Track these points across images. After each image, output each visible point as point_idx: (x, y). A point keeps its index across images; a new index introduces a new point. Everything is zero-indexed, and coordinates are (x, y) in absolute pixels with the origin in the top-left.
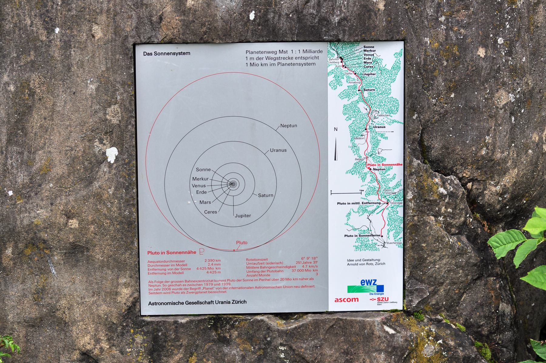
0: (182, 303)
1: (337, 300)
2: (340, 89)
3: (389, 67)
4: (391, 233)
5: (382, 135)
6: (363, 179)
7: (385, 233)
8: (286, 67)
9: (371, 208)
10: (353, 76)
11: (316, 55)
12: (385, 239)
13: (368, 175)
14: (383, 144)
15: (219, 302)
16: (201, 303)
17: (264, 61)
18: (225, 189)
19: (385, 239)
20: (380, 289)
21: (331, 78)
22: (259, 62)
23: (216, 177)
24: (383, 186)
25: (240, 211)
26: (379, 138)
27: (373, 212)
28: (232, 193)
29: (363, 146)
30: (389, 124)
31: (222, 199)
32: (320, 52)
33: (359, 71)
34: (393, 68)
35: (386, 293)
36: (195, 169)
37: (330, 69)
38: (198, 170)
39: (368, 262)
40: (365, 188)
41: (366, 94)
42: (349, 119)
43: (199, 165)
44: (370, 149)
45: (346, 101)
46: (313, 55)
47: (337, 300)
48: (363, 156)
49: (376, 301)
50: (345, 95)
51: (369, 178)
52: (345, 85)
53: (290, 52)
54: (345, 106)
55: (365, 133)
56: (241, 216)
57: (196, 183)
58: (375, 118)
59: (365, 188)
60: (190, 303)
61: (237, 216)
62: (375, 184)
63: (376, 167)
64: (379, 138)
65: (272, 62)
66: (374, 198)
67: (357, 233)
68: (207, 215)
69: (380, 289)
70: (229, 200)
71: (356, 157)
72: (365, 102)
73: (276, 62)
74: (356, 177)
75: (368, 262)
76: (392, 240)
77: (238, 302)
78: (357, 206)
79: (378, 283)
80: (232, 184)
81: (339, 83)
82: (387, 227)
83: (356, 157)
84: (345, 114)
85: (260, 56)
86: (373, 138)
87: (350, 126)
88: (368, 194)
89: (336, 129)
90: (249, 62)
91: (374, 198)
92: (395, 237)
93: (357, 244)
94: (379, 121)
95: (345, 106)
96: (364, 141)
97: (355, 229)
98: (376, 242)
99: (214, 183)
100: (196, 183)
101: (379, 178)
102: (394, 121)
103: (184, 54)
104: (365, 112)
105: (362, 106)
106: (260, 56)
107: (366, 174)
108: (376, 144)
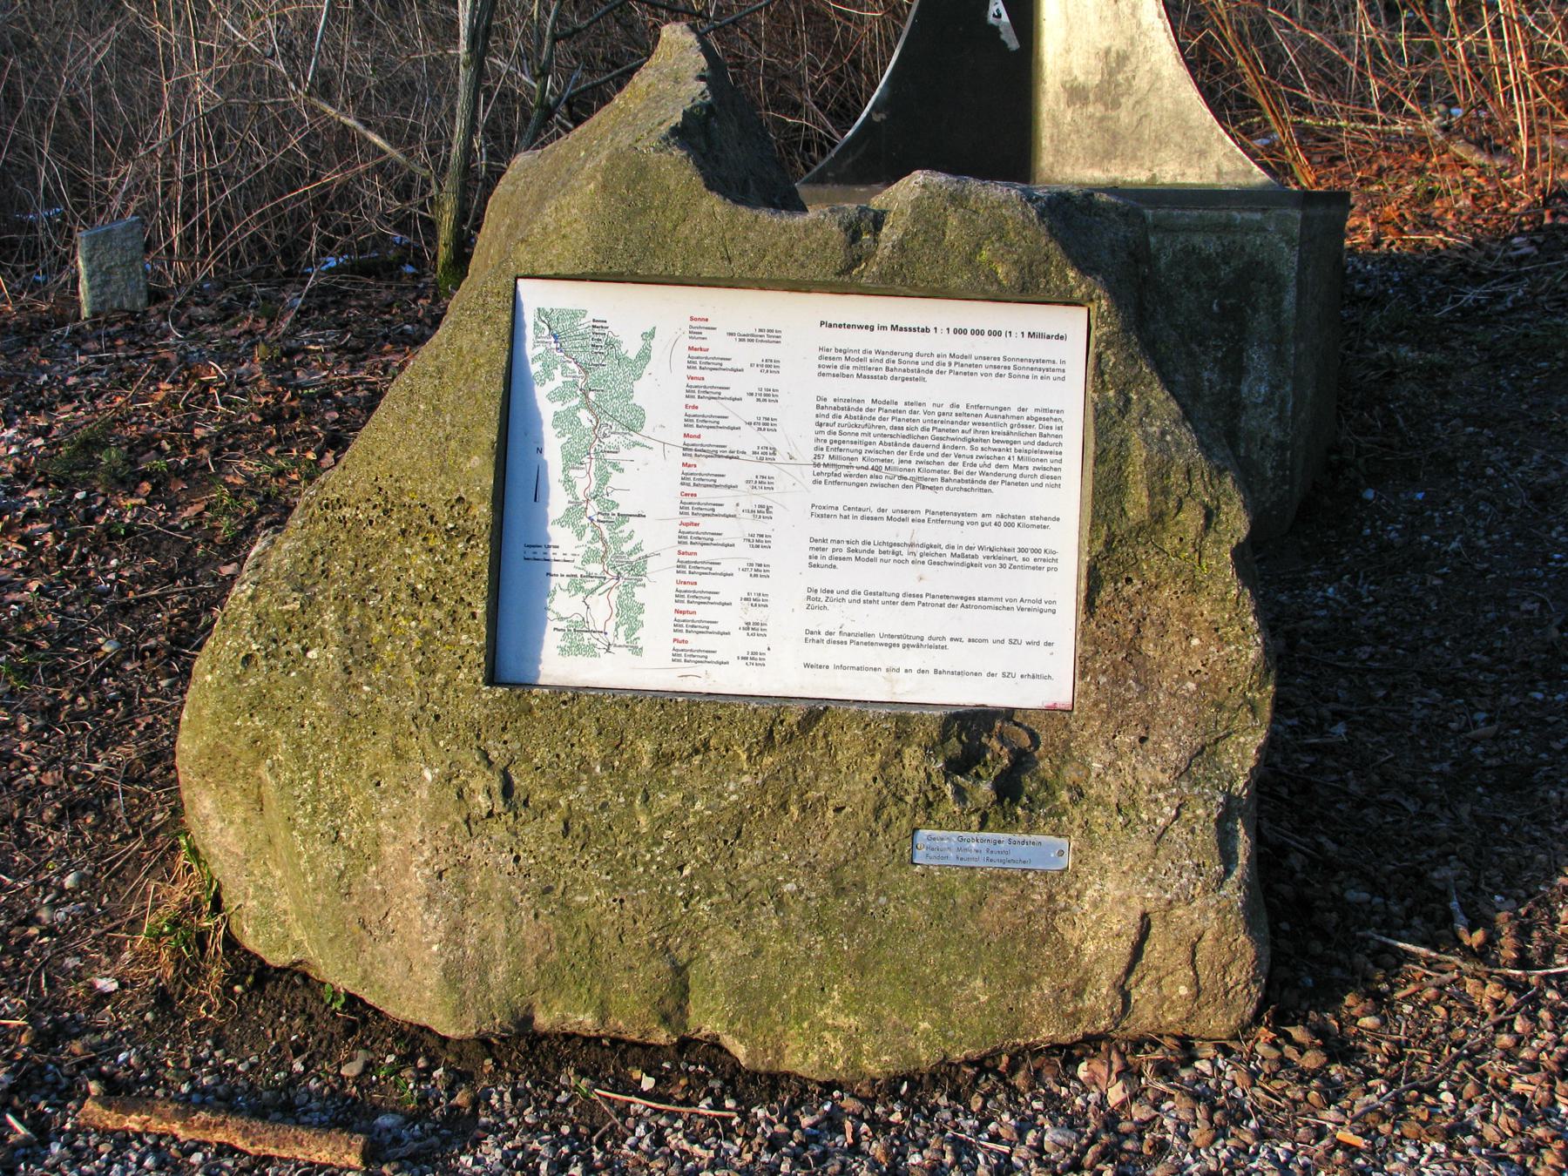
2: (550, 386)
3: (632, 355)
4: (622, 630)
5: (615, 466)
6: (580, 535)
9: (589, 586)
10: (573, 366)
12: (610, 638)
13: (588, 530)
14: (615, 479)
26: (610, 469)
27: (593, 591)
30: (628, 447)
33: (581, 358)
34: (639, 357)
40: (582, 551)
48: (582, 498)
51: (589, 534)
52: (558, 380)
54: (556, 413)
55: (586, 460)
58: (605, 436)
62: (599, 545)
64: (610, 469)
66: (595, 568)
71: (570, 498)
72: (590, 409)
76: (622, 640)
82: (614, 620)
83: (570, 498)
84: (555, 427)
86: (599, 468)
87: (563, 447)
88: (586, 561)
91: (595, 568)
95: (556, 413)
97: (561, 619)
98: (593, 641)
101: (606, 535)
104: (587, 425)
105: (584, 415)
107: (584, 527)
108: (604, 479)
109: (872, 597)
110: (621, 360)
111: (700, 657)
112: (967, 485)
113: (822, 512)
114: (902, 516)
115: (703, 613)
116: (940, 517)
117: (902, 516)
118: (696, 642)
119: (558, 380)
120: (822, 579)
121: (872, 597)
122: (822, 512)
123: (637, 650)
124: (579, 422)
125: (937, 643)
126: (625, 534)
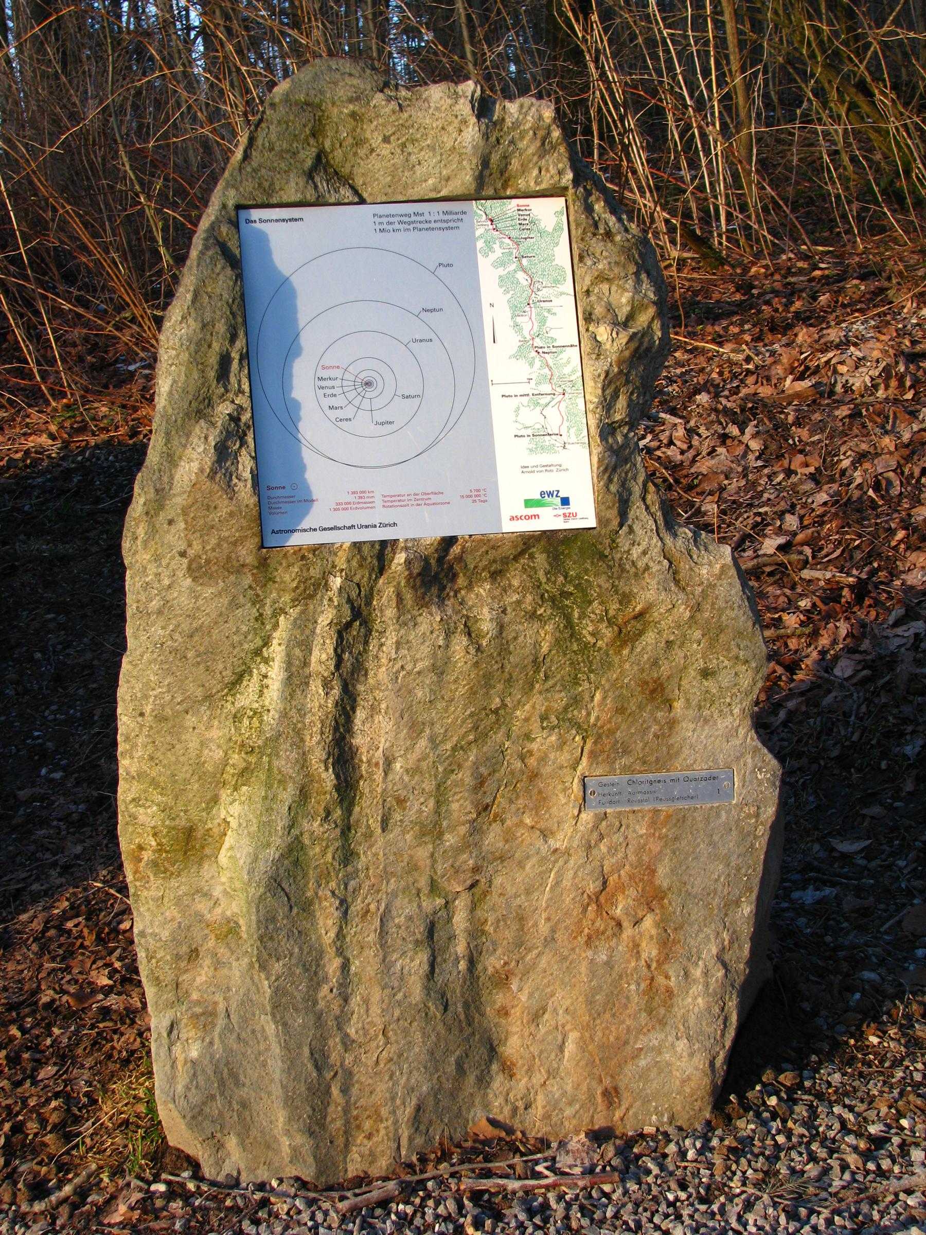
0: (315, 530)
1: (512, 518)
2: (493, 257)
3: (550, 229)
4: (572, 431)
5: (549, 311)
6: (531, 364)
7: (564, 431)
8: (424, 232)
9: (544, 400)
10: (507, 241)
11: (460, 216)
12: (564, 438)
13: (537, 360)
14: (551, 322)
15: (362, 526)
16: (340, 528)
17: (397, 226)
18: (359, 390)
19: (564, 438)
20: (565, 501)
21: (480, 244)
22: (390, 227)
23: (347, 376)
24: (556, 374)
25: (380, 416)
26: (546, 314)
27: (547, 405)
28: (368, 395)
30: (557, 296)
31: (356, 402)
32: (464, 213)
33: (513, 234)
34: (554, 229)
35: (573, 507)
36: (320, 367)
37: (478, 233)
38: (324, 368)
39: (548, 468)
40: (534, 376)
41: (525, 262)
42: (506, 292)
43: (327, 361)
44: (535, 329)
46: (455, 217)
47: (512, 518)
48: (528, 338)
49: (562, 518)
51: (537, 364)
52: (498, 252)
53: (427, 214)
54: (500, 277)
55: (527, 309)
56: (382, 424)
57: (324, 383)
59: (534, 376)
60: (325, 529)
61: (377, 423)
62: (546, 370)
63: (546, 350)
64: (546, 314)
65: (406, 226)
66: (546, 388)
67: (529, 432)
68: (339, 424)
69: (565, 501)
70: (366, 404)
73: (411, 227)
74: (522, 363)
75: (548, 468)
76: (573, 439)
77: (386, 525)
78: (526, 399)
79: (562, 495)
80: (368, 384)
81: (491, 249)
82: (566, 424)
83: (520, 338)
84: (501, 287)
85: (391, 220)
86: (538, 314)
88: (538, 383)
89: (492, 305)
90: (378, 227)
91: (546, 388)
92: (577, 436)
93: (530, 446)
94: (544, 293)
95: (500, 277)
96: (526, 319)
98: (553, 442)
99: (345, 383)
100: (324, 383)
101: (551, 364)
102: (562, 294)
103: (296, 220)
104: (525, 283)
105: (521, 276)
106: (391, 220)
108: (543, 321)
110: (541, 233)
119: (498, 252)
124: (518, 282)
126: (564, 361)
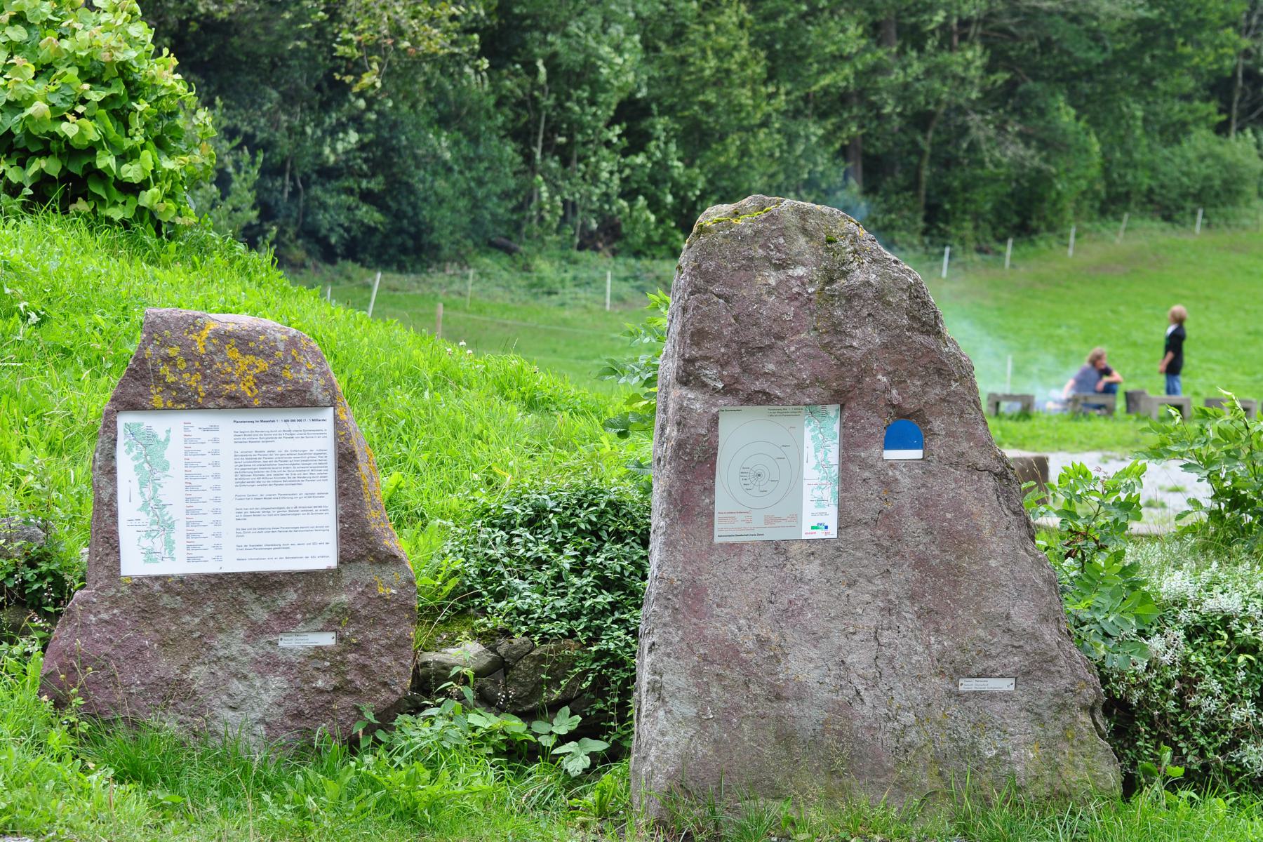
14: (160, 491)
29: (148, 493)
45: (136, 463)
50: (136, 458)
52: (135, 451)
66: (155, 527)
91: (155, 527)
105: (146, 465)
108: (155, 491)
109: (261, 531)
111: (197, 560)
112: (294, 483)
113: (239, 498)
114: (270, 497)
115: (198, 542)
116: (283, 496)
117: (270, 497)
118: (195, 553)
119: (135, 451)
120: (242, 524)
121: (261, 531)
122: (239, 498)
123: (173, 559)
125: (286, 547)
